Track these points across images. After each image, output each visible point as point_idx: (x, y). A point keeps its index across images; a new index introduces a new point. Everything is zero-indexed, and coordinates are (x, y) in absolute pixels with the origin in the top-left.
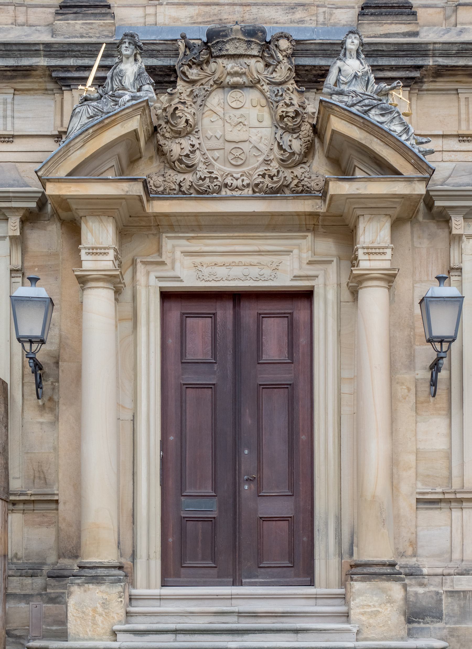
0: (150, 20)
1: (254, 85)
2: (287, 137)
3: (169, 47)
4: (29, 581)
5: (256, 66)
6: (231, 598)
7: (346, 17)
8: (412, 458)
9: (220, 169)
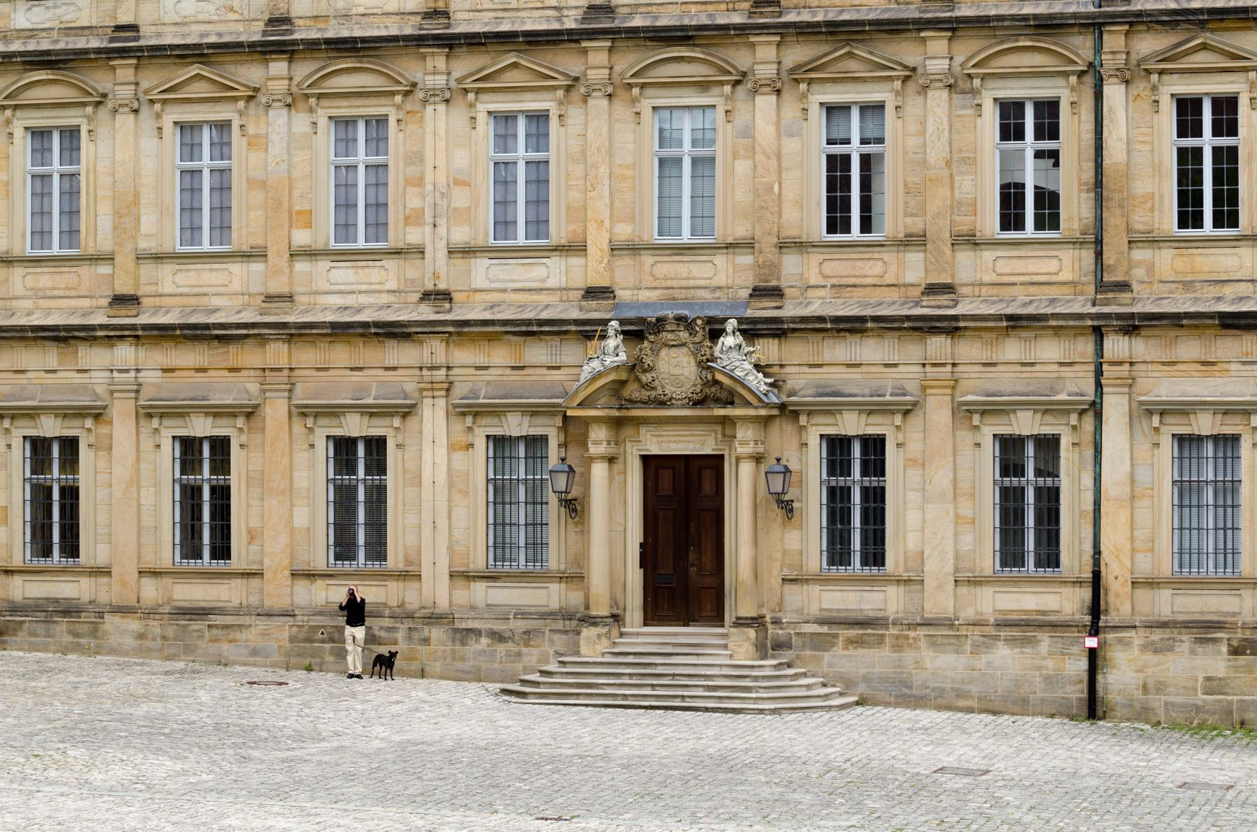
0: (635, 298)
1: (684, 345)
2: (704, 372)
3: (642, 321)
4: (568, 622)
5: (684, 335)
6: (676, 634)
7: (744, 294)
8: (779, 555)
9: (669, 390)
